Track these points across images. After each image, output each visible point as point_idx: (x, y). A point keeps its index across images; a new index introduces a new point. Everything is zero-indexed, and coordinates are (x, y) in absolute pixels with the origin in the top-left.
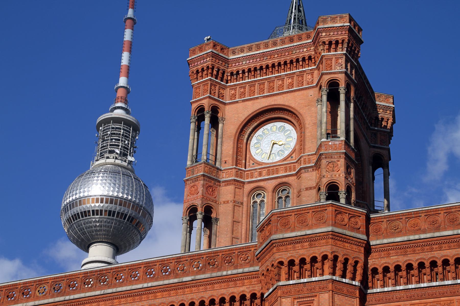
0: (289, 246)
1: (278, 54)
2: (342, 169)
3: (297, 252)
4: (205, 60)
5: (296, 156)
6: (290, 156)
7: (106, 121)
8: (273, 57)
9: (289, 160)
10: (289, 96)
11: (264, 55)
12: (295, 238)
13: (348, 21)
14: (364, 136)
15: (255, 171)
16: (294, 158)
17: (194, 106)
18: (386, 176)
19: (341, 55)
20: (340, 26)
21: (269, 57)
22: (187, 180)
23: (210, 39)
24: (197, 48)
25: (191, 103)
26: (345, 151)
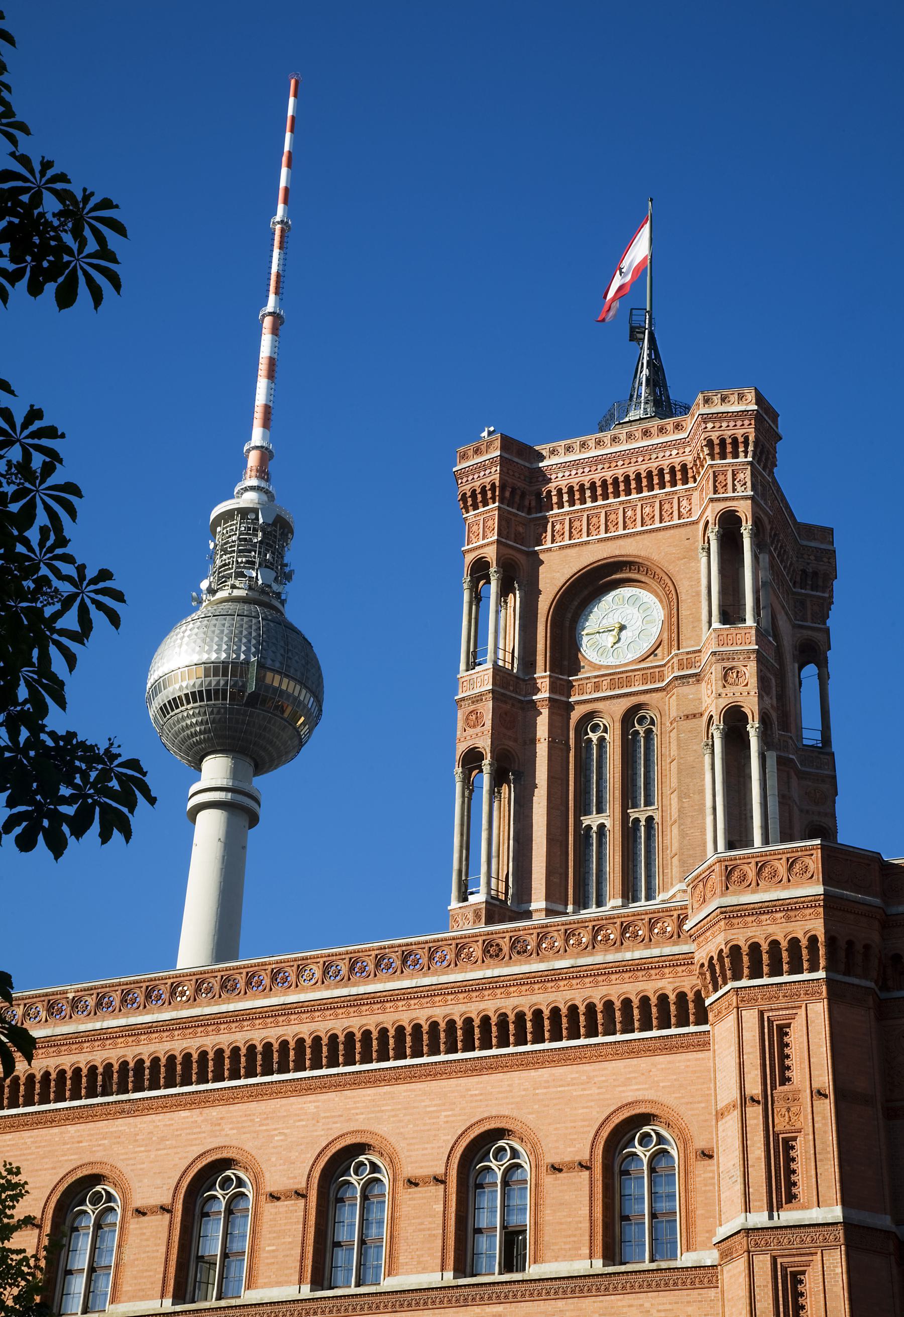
0: (750, 919)
1: (624, 461)
2: (752, 681)
3: (764, 930)
4: (488, 471)
5: (663, 654)
6: (653, 653)
7: (228, 515)
8: (614, 464)
9: (651, 661)
10: (647, 539)
11: (597, 461)
12: (760, 905)
13: (754, 401)
14: (783, 607)
15: (588, 681)
16: (659, 657)
17: (469, 558)
18: (823, 679)
19: (744, 464)
20: (740, 411)
21: (607, 465)
22: (463, 699)
23: (494, 431)
24: (472, 448)
25: (464, 553)
26: (757, 647)
